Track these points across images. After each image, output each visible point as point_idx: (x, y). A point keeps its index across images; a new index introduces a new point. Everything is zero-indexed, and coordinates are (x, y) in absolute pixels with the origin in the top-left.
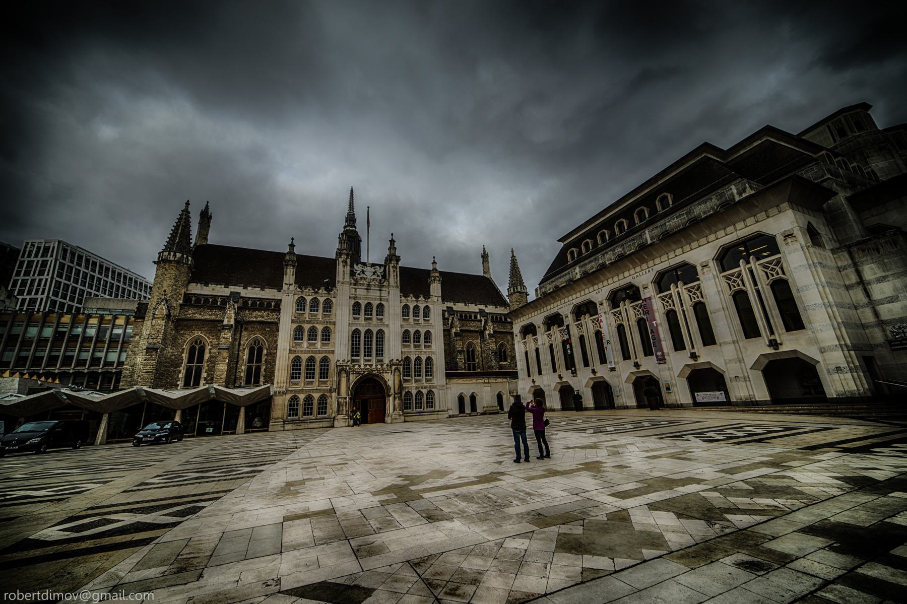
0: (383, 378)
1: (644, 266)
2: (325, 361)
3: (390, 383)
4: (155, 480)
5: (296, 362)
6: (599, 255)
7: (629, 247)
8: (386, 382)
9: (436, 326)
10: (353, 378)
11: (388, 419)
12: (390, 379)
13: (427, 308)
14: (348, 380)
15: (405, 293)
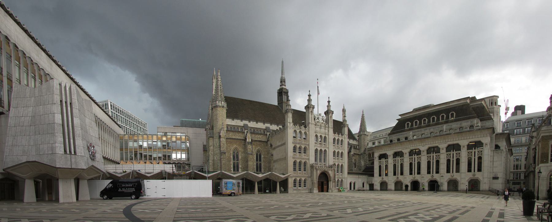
0: (328, 173)
1: (444, 141)
2: (305, 163)
3: (331, 175)
4: (109, 211)
5: (295, 163)
6: (423, 129)
7: (435, 129)
8: (329, 175)
9: (345, 150)
10: (319, 172)
11: (330, 190)
12: (331, 173)
13: (342, 140)
14: (317, 173)
15: (334, 133)
